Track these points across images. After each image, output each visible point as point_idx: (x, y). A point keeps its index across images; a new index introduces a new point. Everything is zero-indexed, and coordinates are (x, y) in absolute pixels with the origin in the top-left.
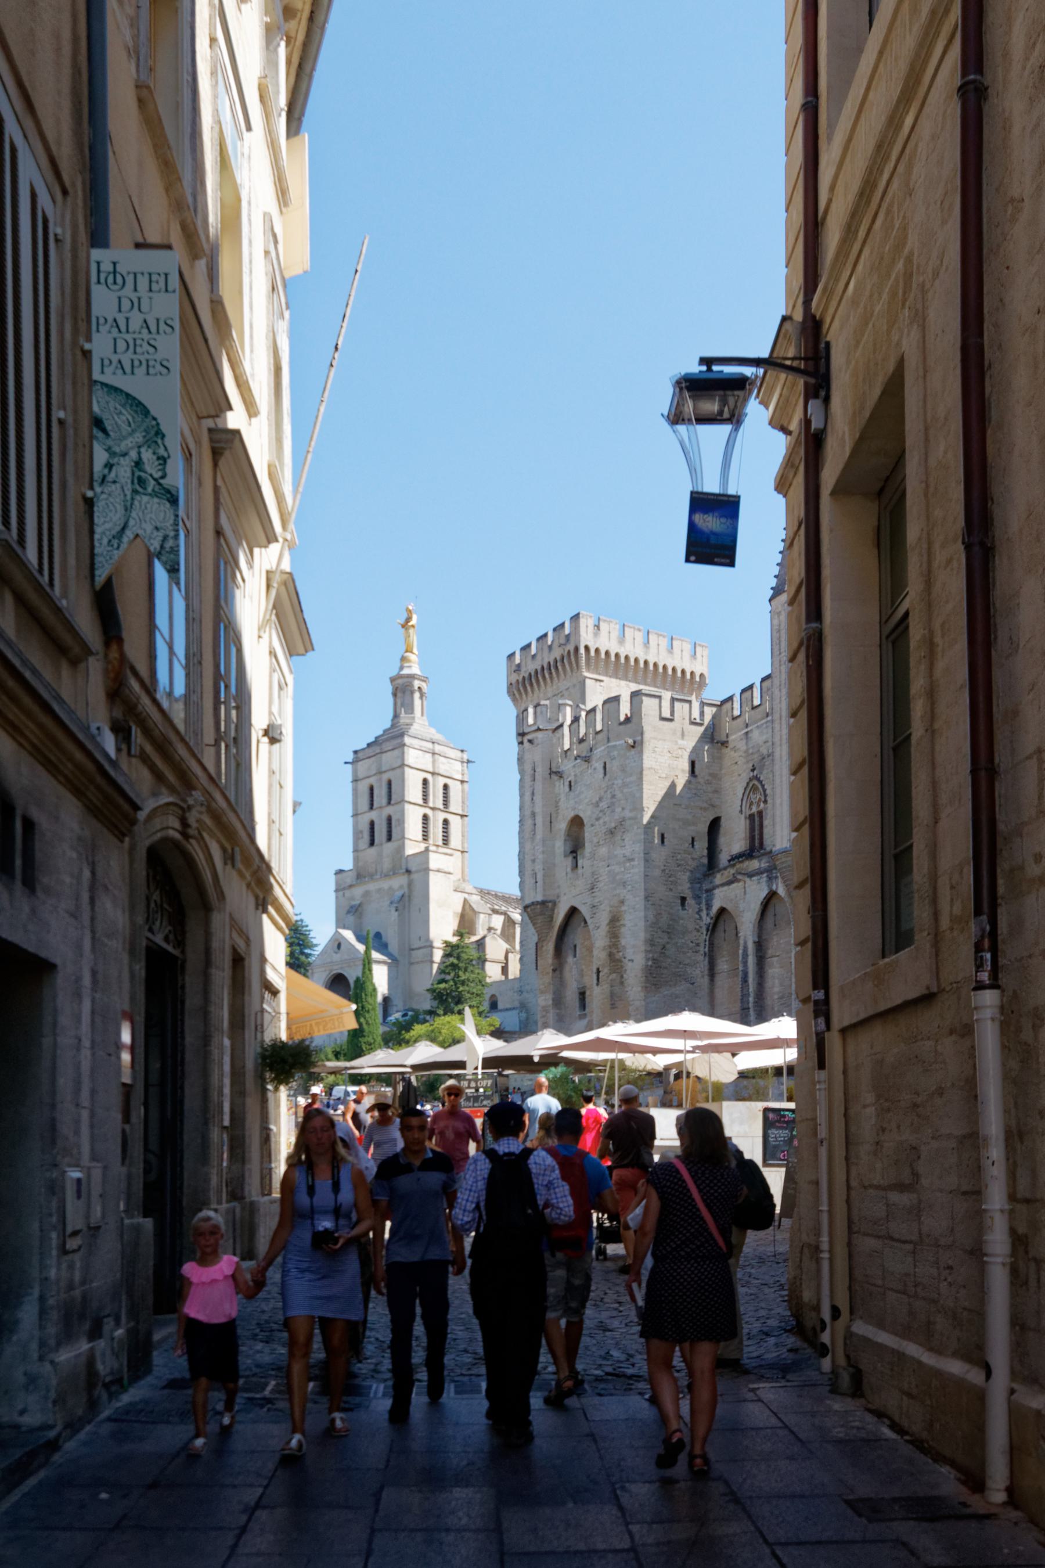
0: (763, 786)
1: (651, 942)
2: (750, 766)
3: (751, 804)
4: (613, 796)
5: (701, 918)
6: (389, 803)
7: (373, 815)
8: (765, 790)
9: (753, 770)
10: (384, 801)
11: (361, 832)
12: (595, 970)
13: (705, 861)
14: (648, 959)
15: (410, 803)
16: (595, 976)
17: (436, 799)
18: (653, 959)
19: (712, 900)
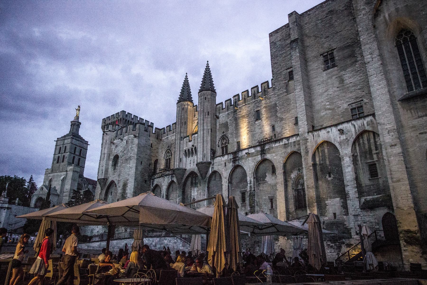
0: (171, 152)
2: (167, 146)
3: (167, 156)
4: (128, 150)
6: (65, 152)
7: (60, 155)
8: (171, 153)
9: (168, 147)
10: (63, 152)
13: (153, 171)
17: (77, 153)
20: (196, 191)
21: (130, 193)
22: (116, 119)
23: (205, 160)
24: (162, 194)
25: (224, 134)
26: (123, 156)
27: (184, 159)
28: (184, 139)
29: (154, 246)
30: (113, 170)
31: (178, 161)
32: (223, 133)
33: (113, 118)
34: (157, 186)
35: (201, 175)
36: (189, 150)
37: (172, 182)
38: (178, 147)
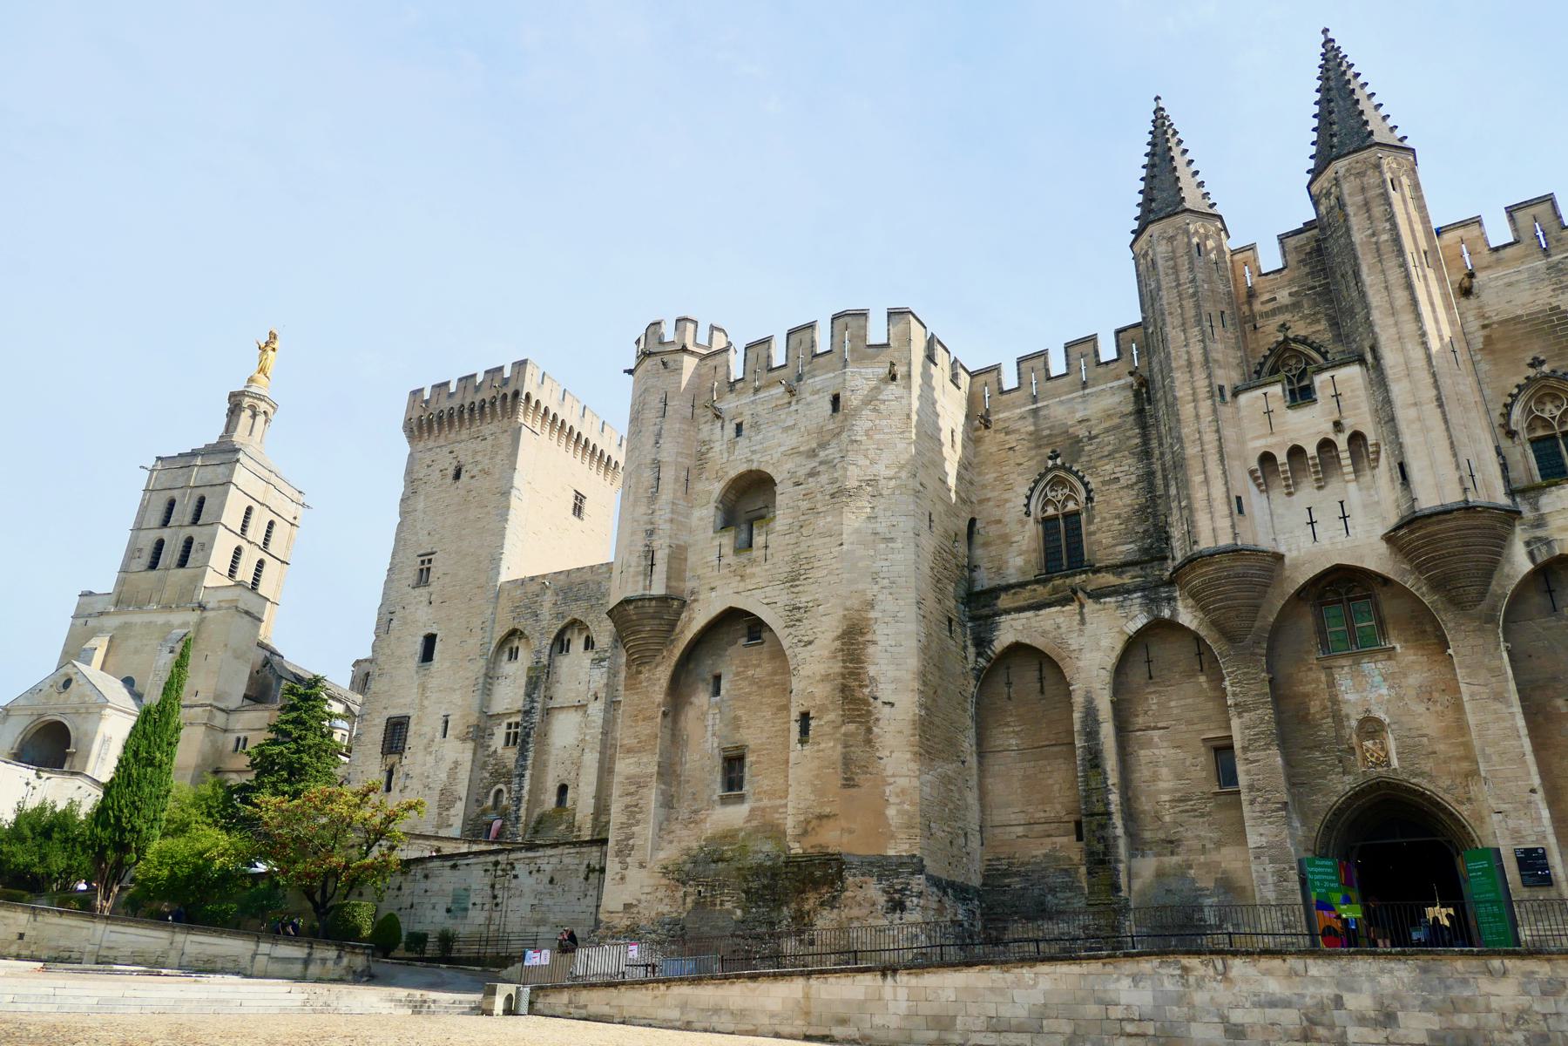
0: (1081, 479)
1: (923, 675)
2: (1048, 451)
3: (1047, 503)
5: (966, 658)
7: (166, 534)
8: (1086, 485)
9: (1054, 456)
11: (140, 550)
12: (795, 714)
14: (921, 705)
15: (226, 527)
16: (795, 728)
17: (256, 531)
18: (927, 708)
19: (992, 631)
20: (1378, 679)
21: (895, 680)
22: (487, 395)
23: (1477, 498)
24: (1078, 699)
25: (1546, 368)
26: (812, 474)
27: (1255, 501)
28: (1244, 398)
29: (1362, 1020)
30: (728, 550)
31: (1221, 508)
32: (1536, 363)
33: (470, 388)
34: (1017, 649)
35: (1437, 585)
36: (1296, 452)
37: (1160, 628)
38: (1210, 437)
